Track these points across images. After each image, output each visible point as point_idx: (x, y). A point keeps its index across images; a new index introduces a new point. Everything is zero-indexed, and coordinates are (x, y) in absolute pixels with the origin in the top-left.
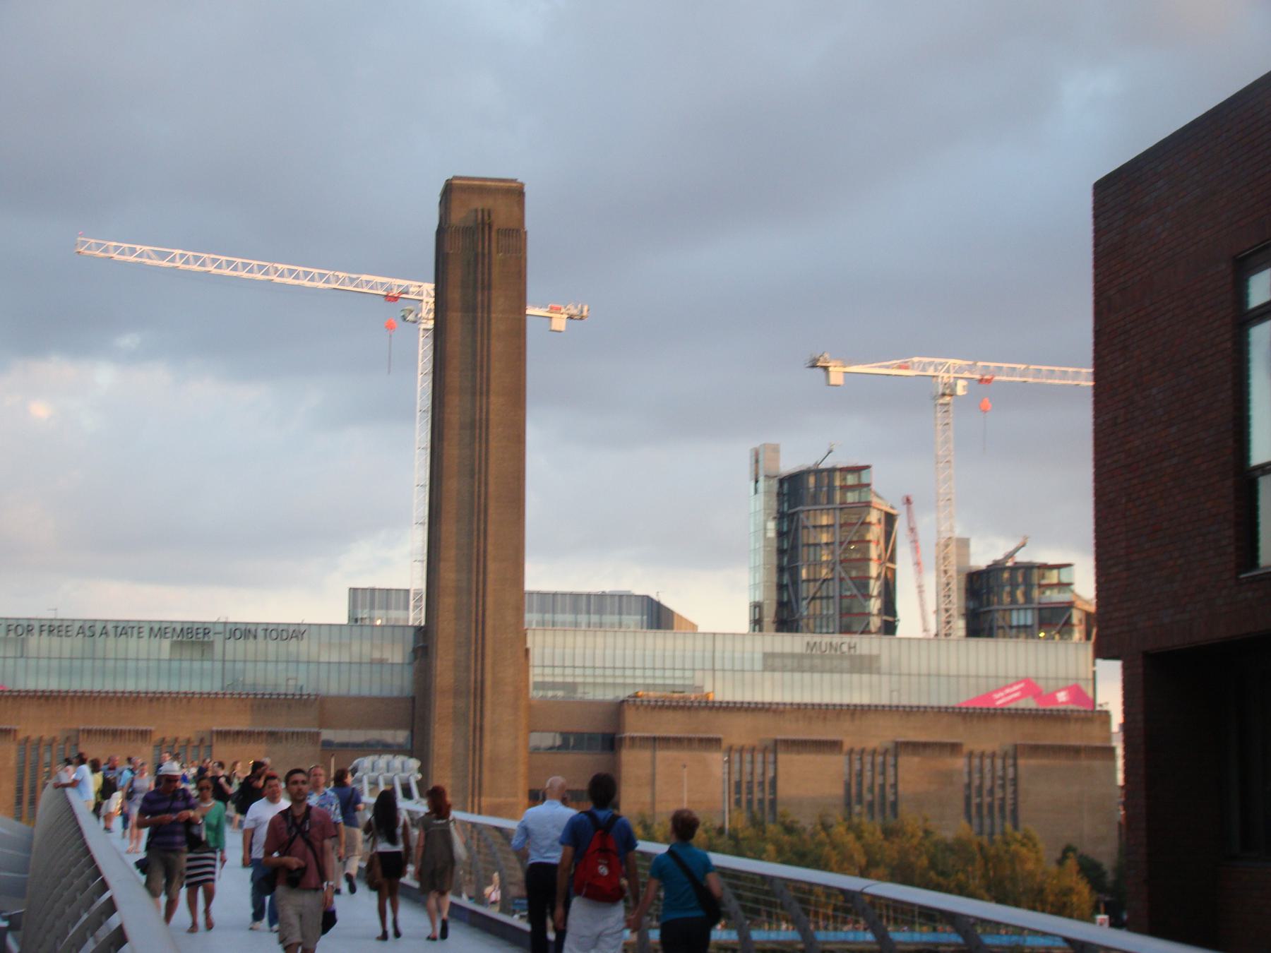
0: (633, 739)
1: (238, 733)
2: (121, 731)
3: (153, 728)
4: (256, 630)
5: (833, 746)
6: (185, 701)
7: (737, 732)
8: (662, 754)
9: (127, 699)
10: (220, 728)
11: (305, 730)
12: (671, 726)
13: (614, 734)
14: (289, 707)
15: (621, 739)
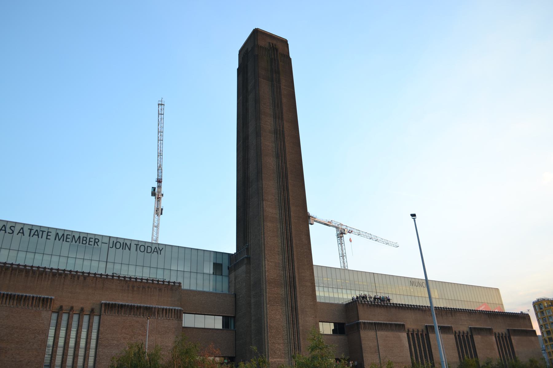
0: (364, 323)
1: (122, 306)
2: (26, 296)
3: (53, 297)
4: (130, 244)
6: (81, 278)
8: (381, 334)
9: (34, 272)
10: (107, 302)
11: (171, 308)
12: (380, 317)
13: (345, 323)
14: (160, 290)
15: (358, 324)
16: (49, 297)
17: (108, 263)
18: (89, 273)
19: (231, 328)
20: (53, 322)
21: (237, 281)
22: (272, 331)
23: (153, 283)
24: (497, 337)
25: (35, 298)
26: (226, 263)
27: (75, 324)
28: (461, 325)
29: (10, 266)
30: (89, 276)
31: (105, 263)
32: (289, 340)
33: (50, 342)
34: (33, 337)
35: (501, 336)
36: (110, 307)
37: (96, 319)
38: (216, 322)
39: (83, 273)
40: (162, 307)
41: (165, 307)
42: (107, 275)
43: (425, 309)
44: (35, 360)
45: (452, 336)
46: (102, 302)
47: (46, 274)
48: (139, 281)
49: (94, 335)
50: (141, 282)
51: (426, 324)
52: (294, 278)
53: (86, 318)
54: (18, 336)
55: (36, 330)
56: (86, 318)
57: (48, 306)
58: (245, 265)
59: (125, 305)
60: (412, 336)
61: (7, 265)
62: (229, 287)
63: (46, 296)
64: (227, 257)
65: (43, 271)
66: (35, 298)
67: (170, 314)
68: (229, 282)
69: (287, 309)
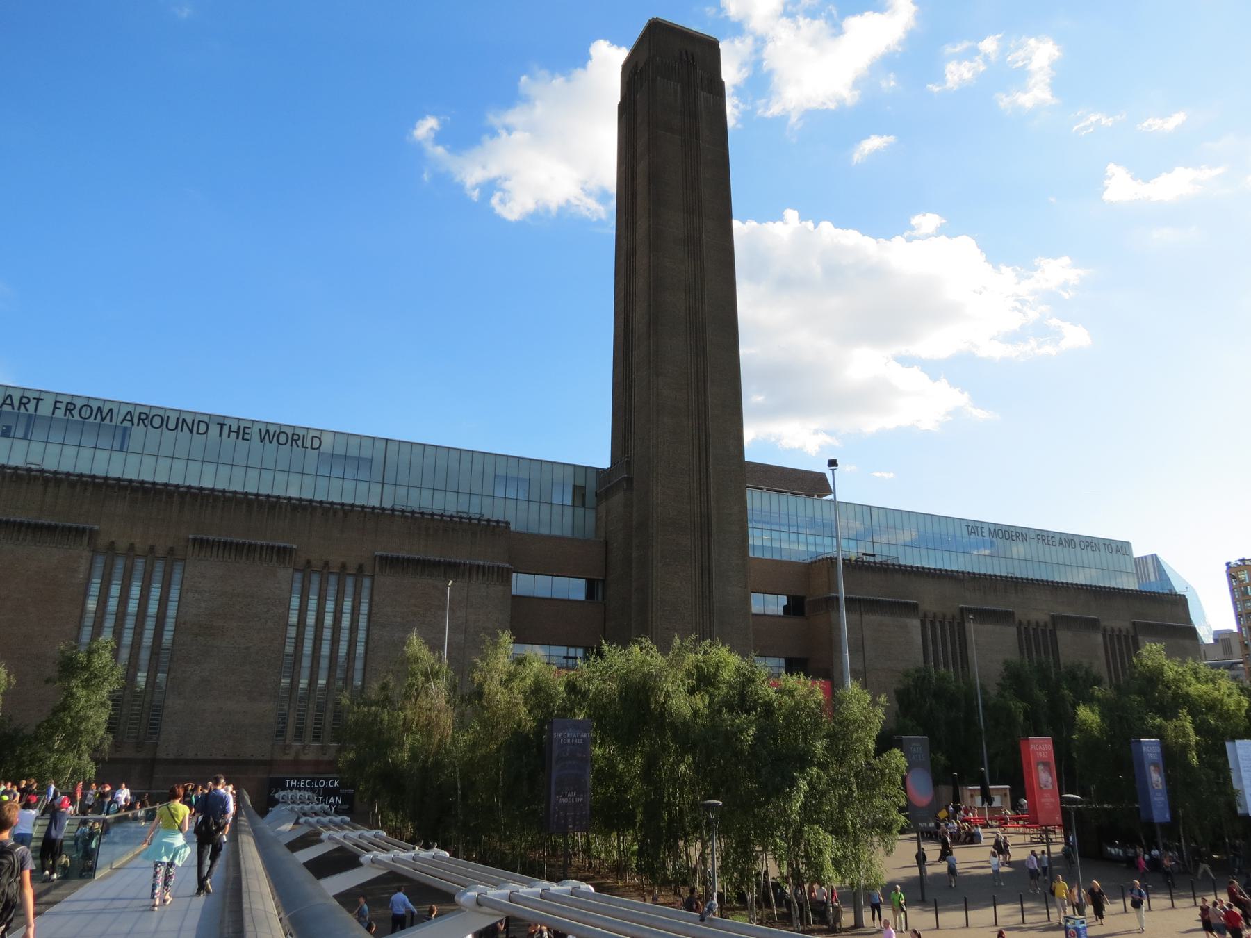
2: (250, 545)
3: (295, 546)
5: (1003, 617)
6: (341, 514)
7: (930, 599)
9: (260, 504)
10: (385, 554)
11: (491, 564)
13: (803, 598)
16: (288, 545)
17: (385, 486)
18: (353, 506)
19: (597, 599)
20: (297, 586)
21: (610, 518)
22: (666, 608)
23: (461, 522)
24: (1108, 637)
25: (265, 548)
26: (592, 485)
27: (332, 590)
28: (1034, 609)
29: (220, 494)
30: (352, 510)
31: (380, 485)
32: (694, 625)
33: (293, 619)
34: (265, 610)
35: (1117, 635)
36: (389, 563)
37: (367, 582)
38: (575, 589)
39: (343, 505)
40: (477, 563)
41: (481, 563)
42: (383, 509)
43: (962, 578)
44: (270, 646)
45: (1012, 630)
46: (376, 553)
47: (281, 508)
48: (437, 519)
49: (364, 608)
50: (441, 520)
51: (961, 606)
52: (708, 517)
53: (350, 582)
54: (242, 608)
55: (269, 598)
56: (350, 582)
57: (287, 561)
58: (623, 493)
59: (414, 560)
60: (930, 623)
61: (216, 493)
62: (597, 528)
63: (283, 545)
64: (594, 474)
65: (276, 502)
66: (265, 548)
67: (490, 575)
68: (597, 519)
69: (693, 572)
